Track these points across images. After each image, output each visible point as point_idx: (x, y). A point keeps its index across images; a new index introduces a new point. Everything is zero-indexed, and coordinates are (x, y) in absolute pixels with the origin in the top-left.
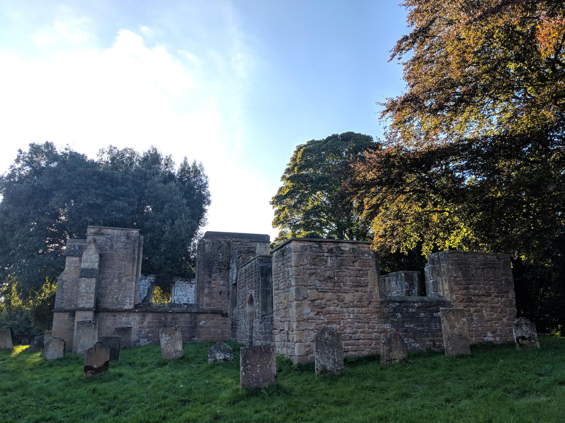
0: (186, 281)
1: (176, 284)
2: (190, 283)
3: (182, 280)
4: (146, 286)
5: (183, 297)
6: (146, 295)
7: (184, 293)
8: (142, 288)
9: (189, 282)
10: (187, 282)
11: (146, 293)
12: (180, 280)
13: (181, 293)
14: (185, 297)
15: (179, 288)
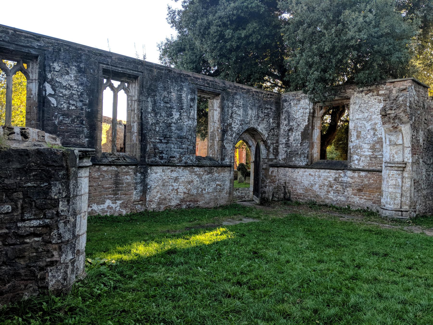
0: (370, 91)
1: (351, 101)
2: (378, 95)
3: (362, 91)
4: (306, 109)
5: (365, 122)
6: (307, 123)
7: (366, 115)
8: (301, 113)
9: (375, 93)
10: (371, 94)
11: (306, 121)
12: (359, 92)
13: (361, 116)
14: (368, 122)
15: (357, 107)
